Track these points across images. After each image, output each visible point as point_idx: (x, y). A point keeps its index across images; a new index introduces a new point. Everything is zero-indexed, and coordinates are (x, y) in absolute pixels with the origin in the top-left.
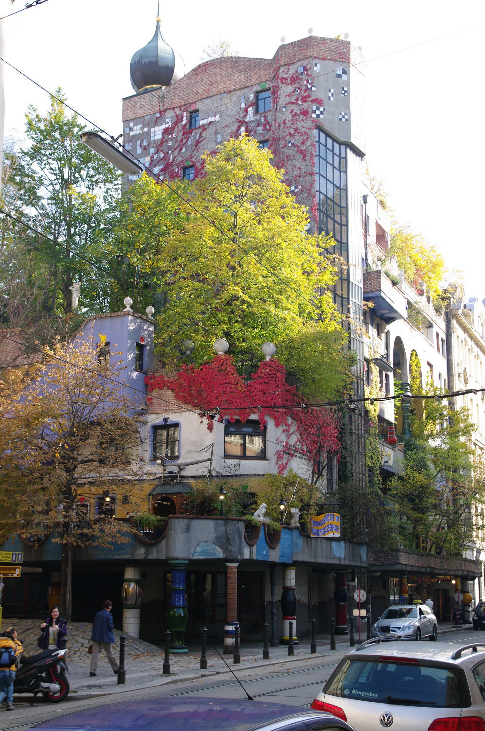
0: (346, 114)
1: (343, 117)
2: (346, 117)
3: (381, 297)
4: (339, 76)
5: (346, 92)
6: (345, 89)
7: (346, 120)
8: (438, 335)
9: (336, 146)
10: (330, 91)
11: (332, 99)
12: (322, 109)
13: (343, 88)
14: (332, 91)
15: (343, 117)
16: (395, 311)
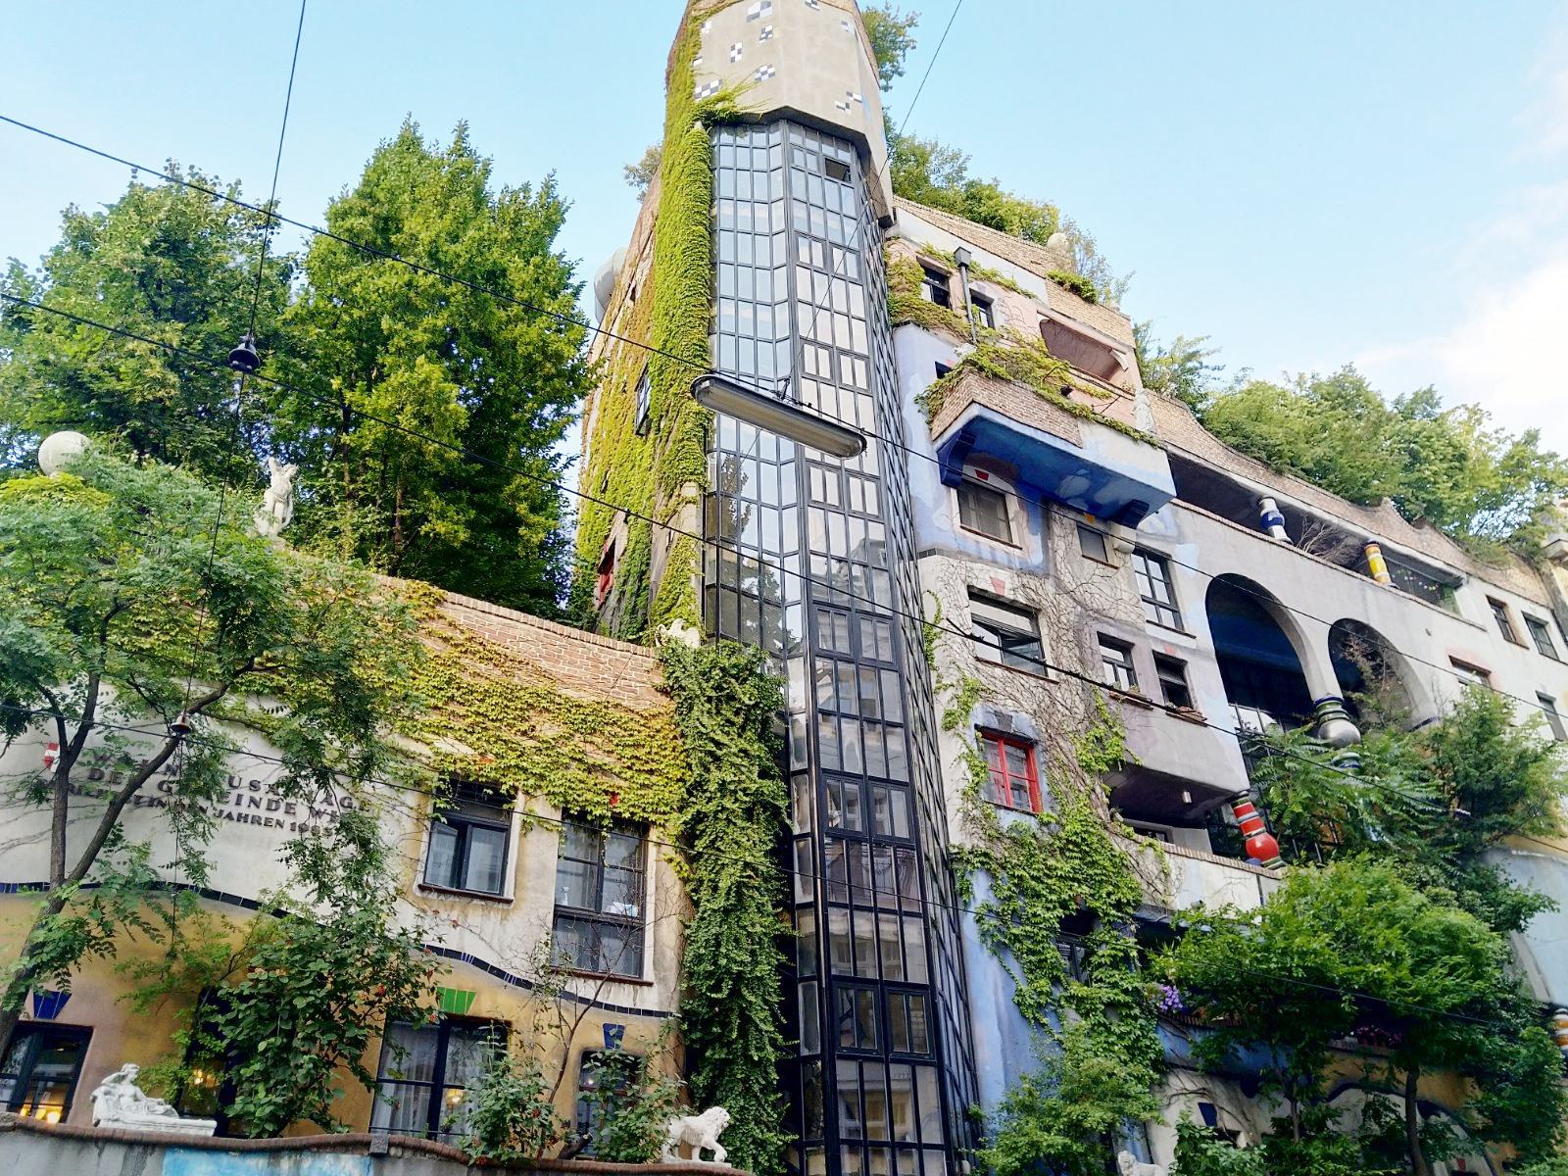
0: (770, 67)
1: (764, 73)
2: (771, 71)
3: (978, 419)
4: (757, 16)
5: (770, 32)
6: (768, 29)
7: (772, 75)
8: (1498, 605)
9: (759, 138)
10: (733, 48)
11: (738, 58)
12: (715, 84)
13: (763, 32)
14: (738, 46)
15: (764, 73)
16: (1099, 475)
